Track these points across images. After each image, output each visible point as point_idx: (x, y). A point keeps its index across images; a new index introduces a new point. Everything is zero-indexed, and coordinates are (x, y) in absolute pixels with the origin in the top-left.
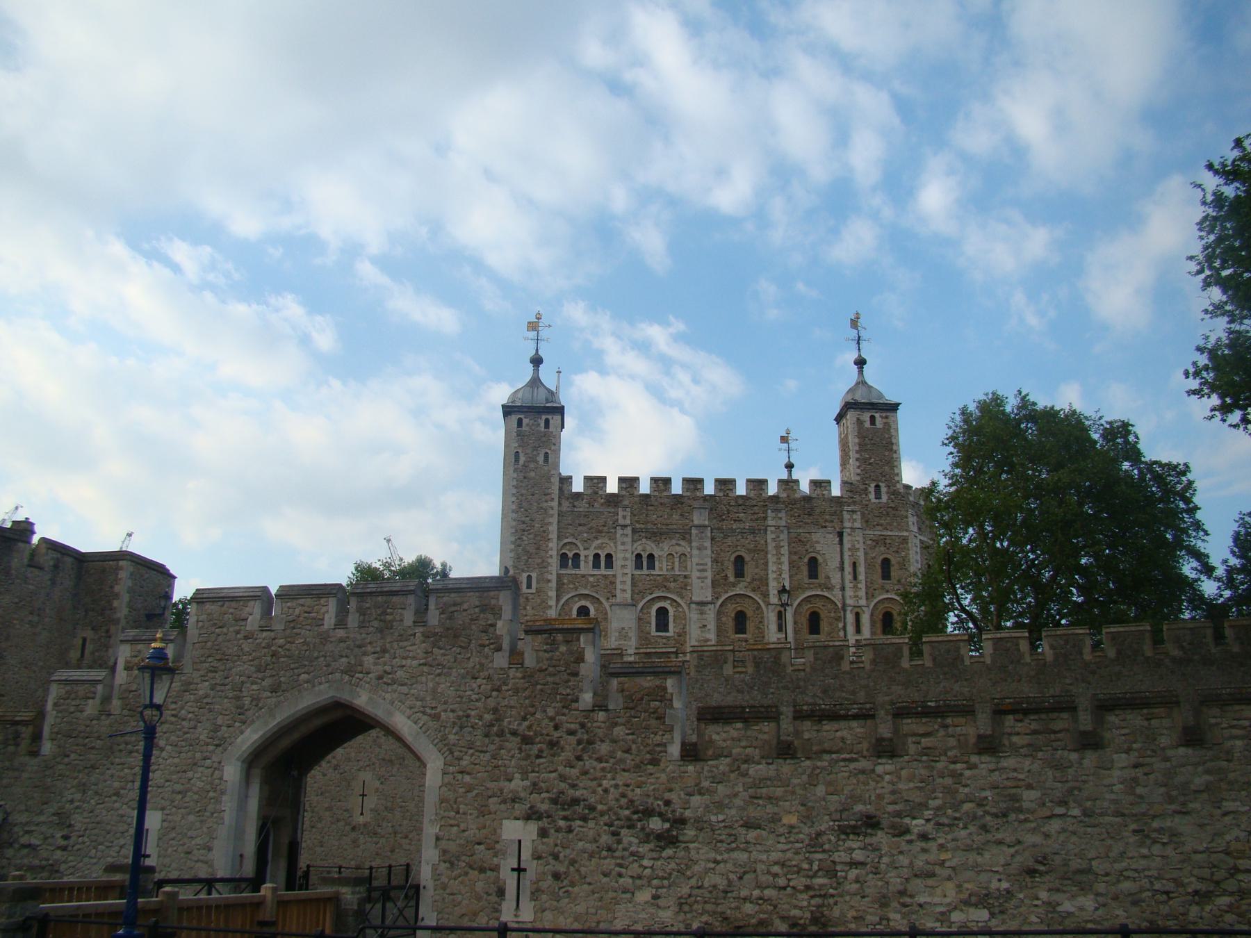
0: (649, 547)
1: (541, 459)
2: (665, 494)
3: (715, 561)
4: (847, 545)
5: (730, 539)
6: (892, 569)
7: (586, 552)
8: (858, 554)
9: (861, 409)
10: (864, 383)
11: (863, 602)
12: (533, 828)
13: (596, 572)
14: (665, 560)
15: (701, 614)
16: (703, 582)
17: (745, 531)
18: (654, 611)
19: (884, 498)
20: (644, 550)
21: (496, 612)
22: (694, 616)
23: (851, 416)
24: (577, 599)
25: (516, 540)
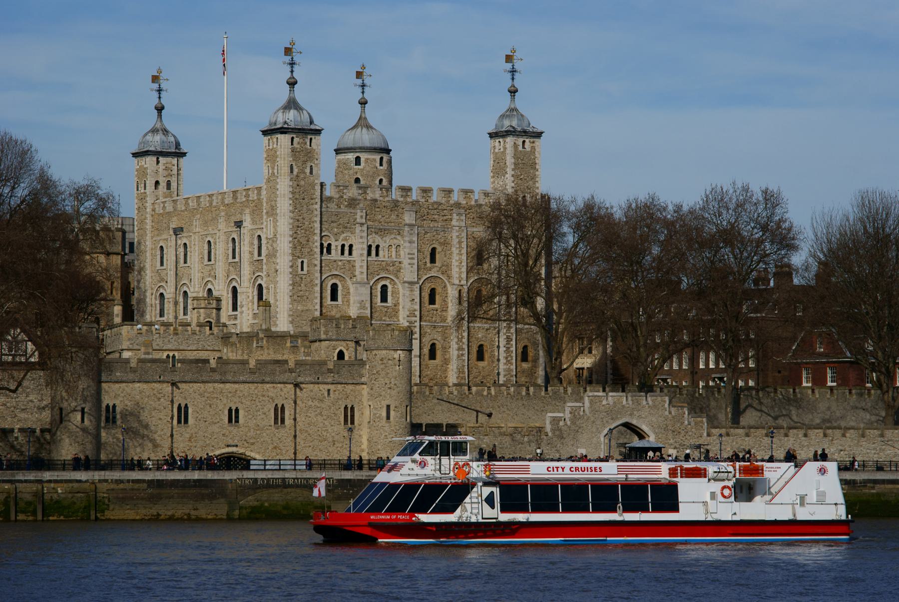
0: (376, 240)
1: (308, 171)
2: (387, 199)
5: (428, 234)
7: (337, 243)
9: (517, 135)
10: (516, 110)
12: (676, 451)
13: (342, 258)
16: (412, 267)
17: (438, 229)
18: (379, 289)
20: (374, 242)
21: (665, 402)
22: (408, 293)
23: (510, 140)
24: (330, 278)
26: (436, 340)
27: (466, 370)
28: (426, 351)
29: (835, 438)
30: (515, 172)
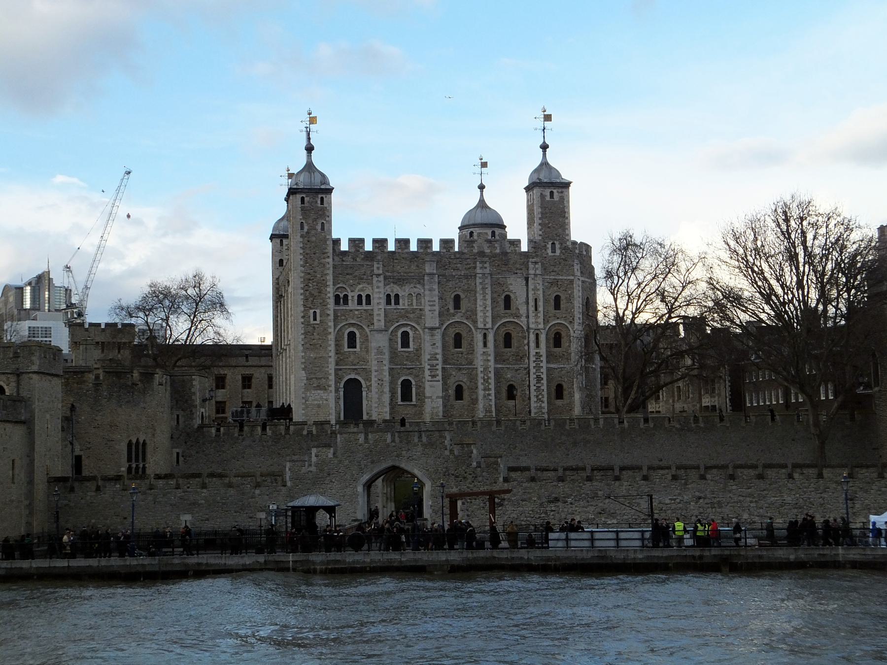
0: (396, 289)
1: (319, 227)
2: (406, 251)
3: (441, 298)
4: (531, 287)
5: (451, 282)
6: (562, 302)
7: (352, 294)
8: (539, 293)
11: (541, 326)
13: (359, 308)
14: (406, 298)
15: (432, 336)
16: (432, 313)
19: (558, 252)
20: (392, 291)
22: (427, 337)
23: (536, 191)
24: (347, 327)
25: (304, 286)
26: (462, 381)
27: (493, 409)
28: (452, 392)
29: (690, 481)
30: (543, 221)
